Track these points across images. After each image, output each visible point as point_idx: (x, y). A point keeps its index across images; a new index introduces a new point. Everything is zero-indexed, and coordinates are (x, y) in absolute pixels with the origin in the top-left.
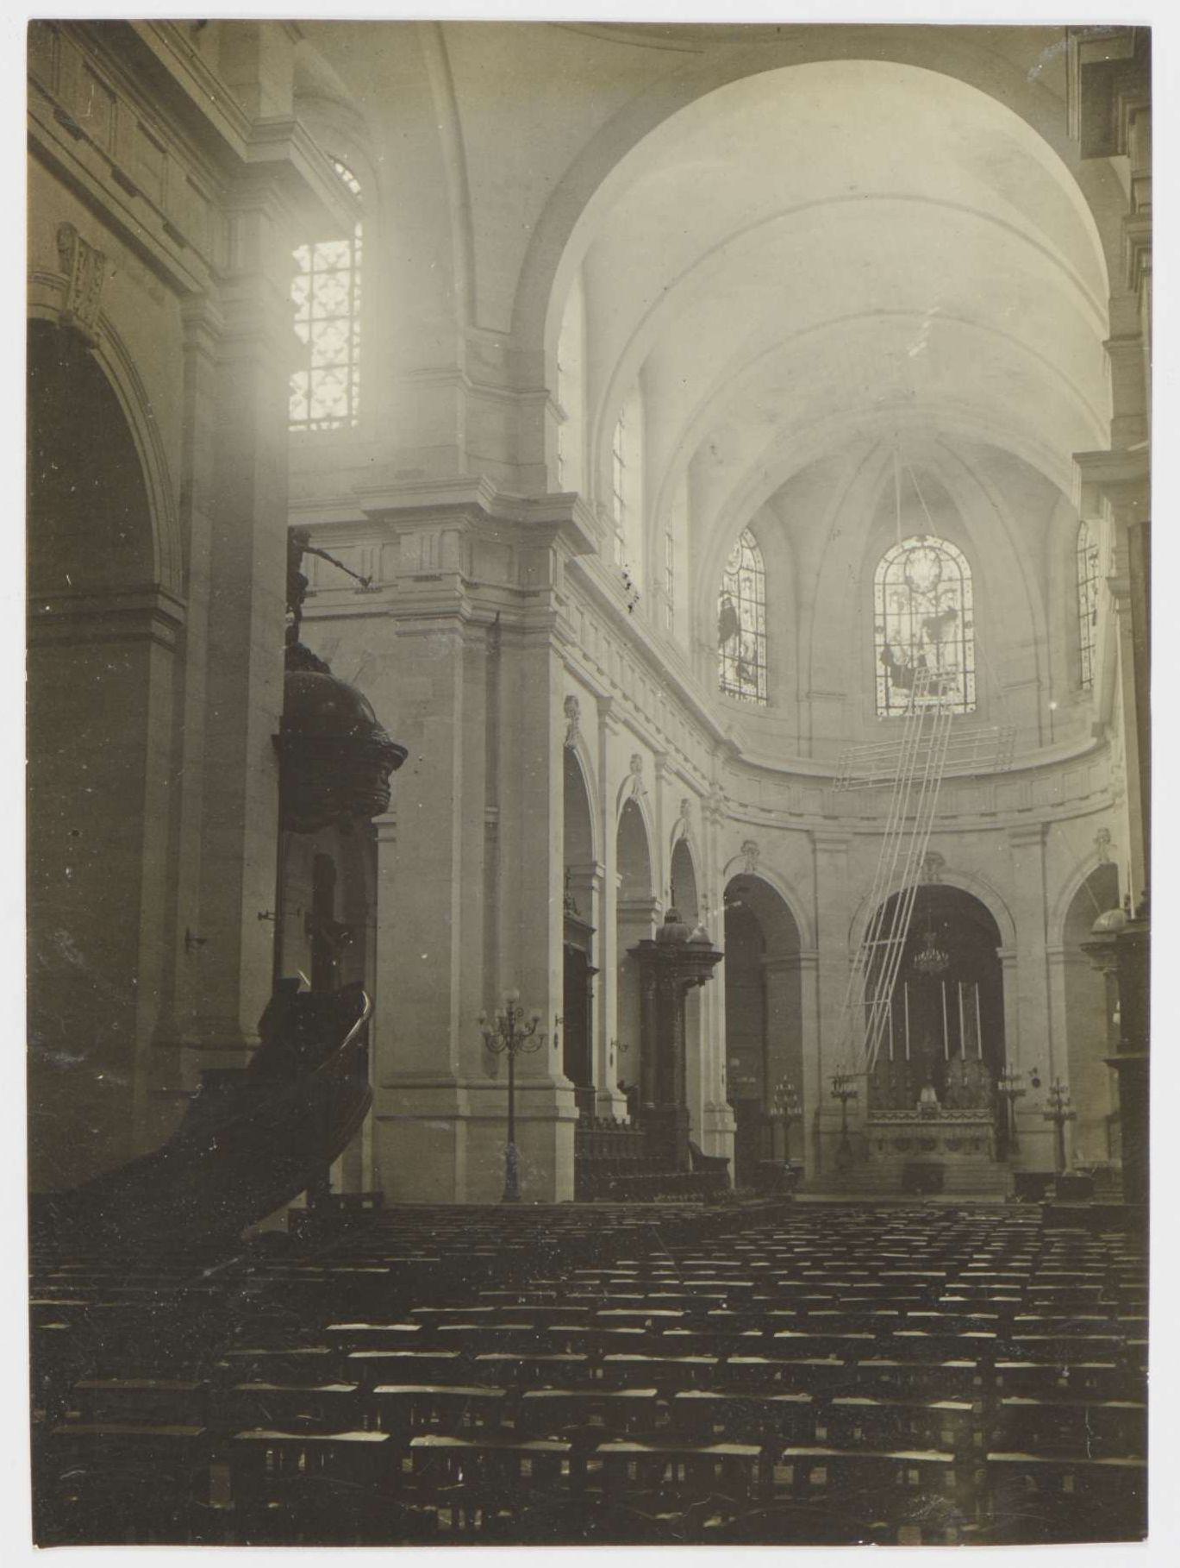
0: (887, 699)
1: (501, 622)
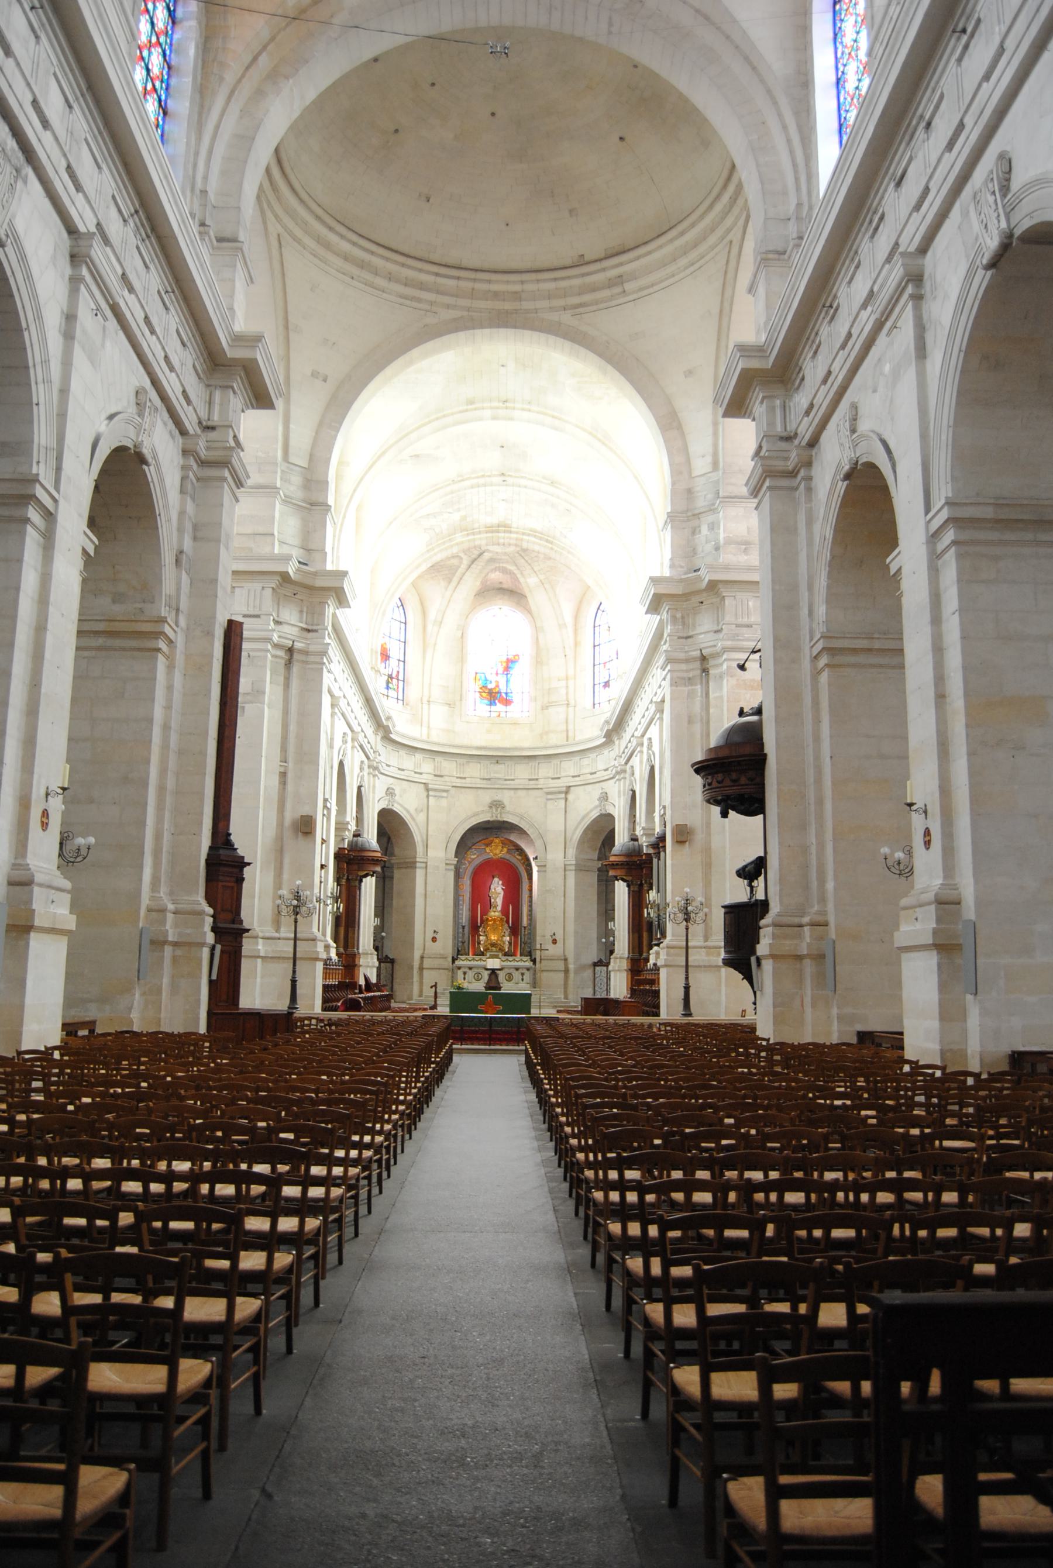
1: (295, 647)
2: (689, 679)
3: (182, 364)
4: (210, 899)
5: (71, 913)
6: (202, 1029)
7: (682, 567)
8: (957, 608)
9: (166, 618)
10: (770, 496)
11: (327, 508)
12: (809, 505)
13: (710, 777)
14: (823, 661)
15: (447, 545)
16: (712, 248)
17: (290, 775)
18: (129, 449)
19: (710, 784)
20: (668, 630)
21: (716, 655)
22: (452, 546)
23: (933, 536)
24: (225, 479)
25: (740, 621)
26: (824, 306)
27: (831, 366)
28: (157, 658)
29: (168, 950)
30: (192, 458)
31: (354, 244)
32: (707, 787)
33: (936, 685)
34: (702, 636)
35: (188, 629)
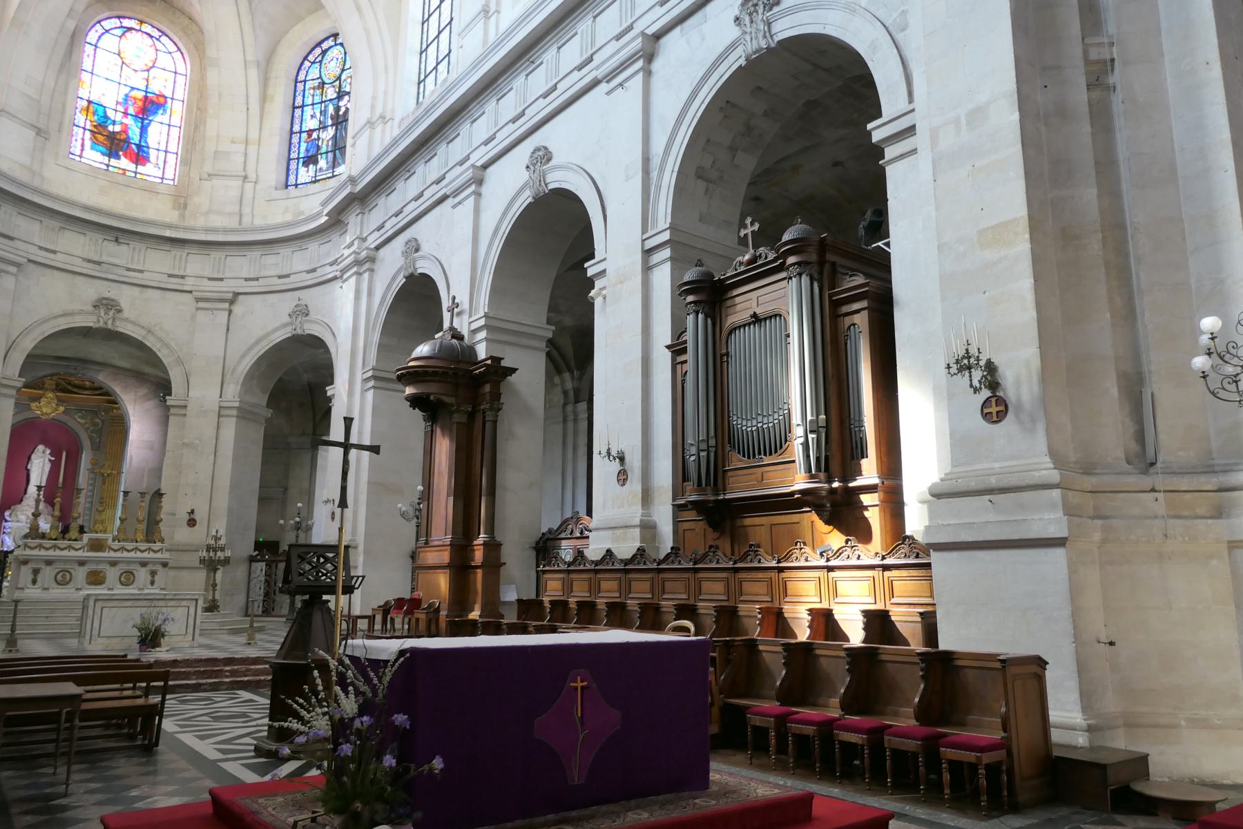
0: (82, 150)
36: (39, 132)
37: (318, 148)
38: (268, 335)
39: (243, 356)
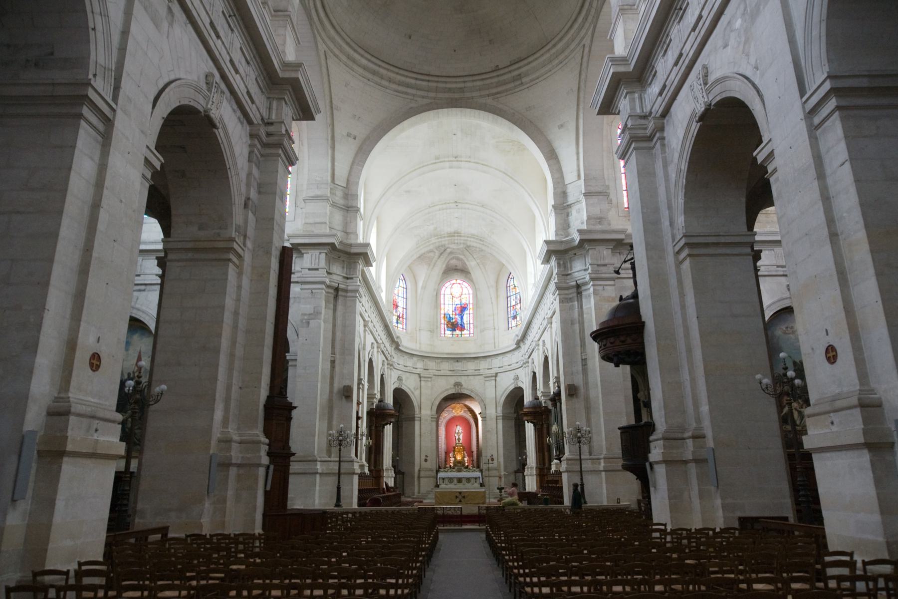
2: (570, 298)
3: (247, 75)
4: (267, 433)
5: (121, 440)
6: (258, 530)
7: (562, 235)
8: (847, 158)
9: (235, 238)
10: (636, 154)
11: (357, 210)
12: (664, 155)
13: (604, 341)
14: (686, 252)
15: (428, 244)
16: (572, 51)
17: (337, 362)
18: (201, 112)
19: (605, 345)
20: (555, 271)
21: (586, 284)
22: (430, 245)
23: (810, 113)
24: (279, 155)
25: (599, 263)
26: (676, 9)
27: (682, 49)
28: (228, 265)
29: (233, 471)
30: (256, 140)
31: (369, 60)
32: (603, 347)
33: (829, 227)
34: (577, 273)
35: (254, 250)
36: (431, 331)
37: (516, 312)
38: (508, 387)
39: (501, 397)
